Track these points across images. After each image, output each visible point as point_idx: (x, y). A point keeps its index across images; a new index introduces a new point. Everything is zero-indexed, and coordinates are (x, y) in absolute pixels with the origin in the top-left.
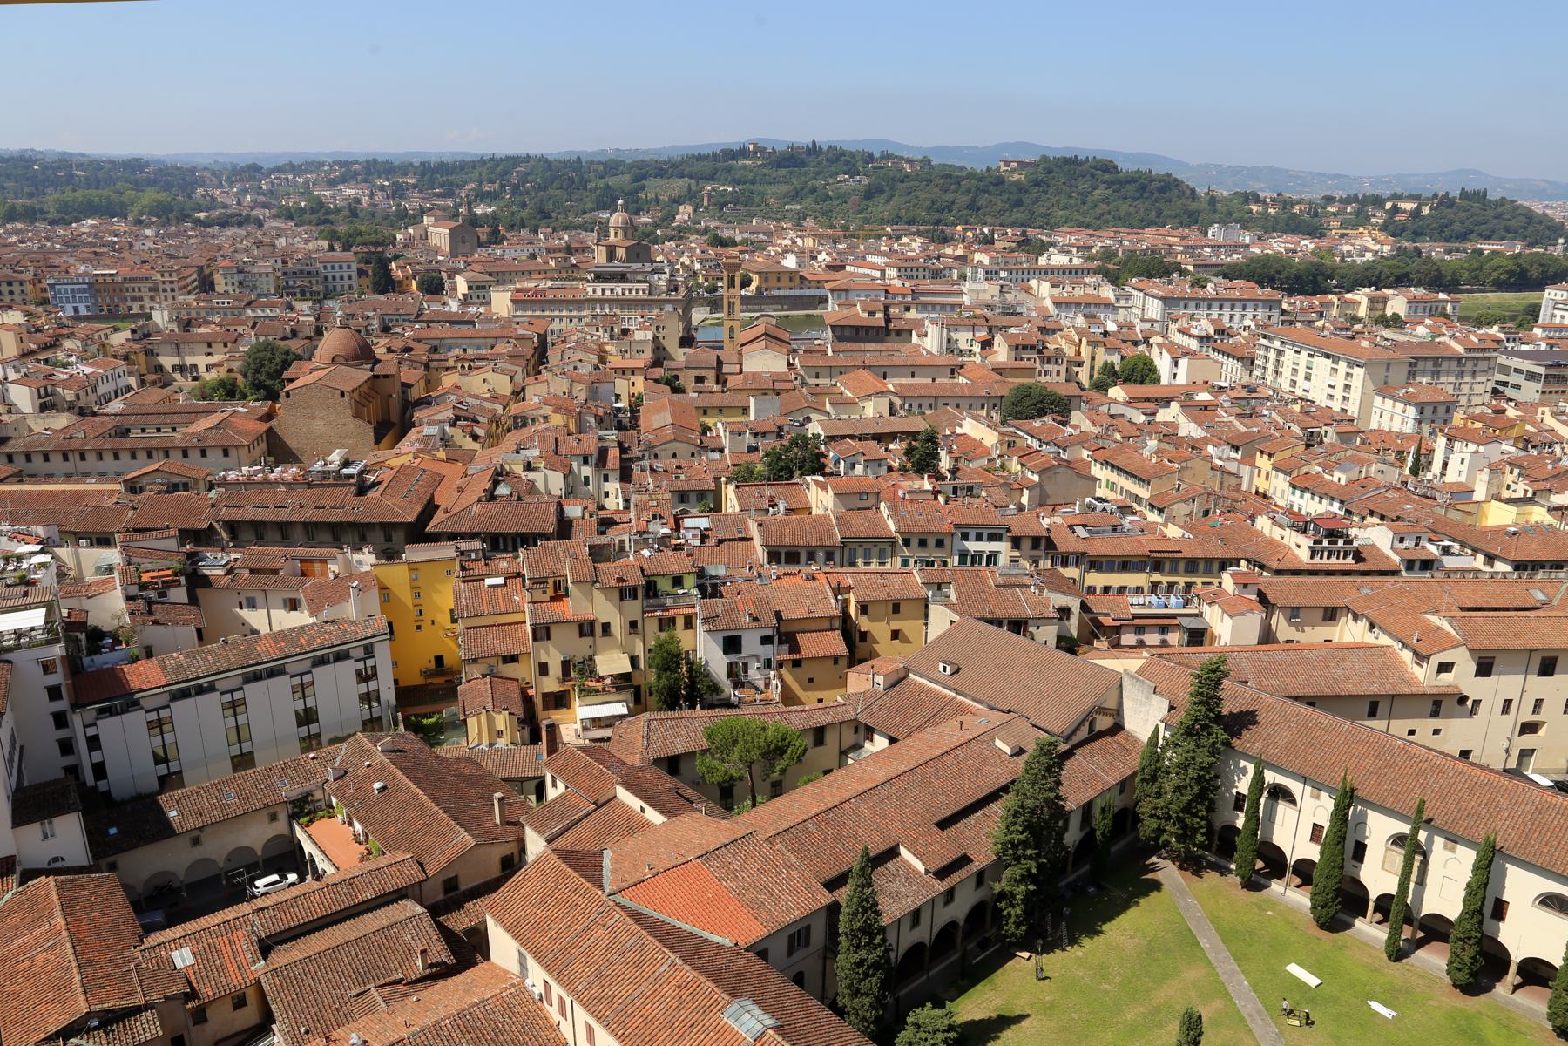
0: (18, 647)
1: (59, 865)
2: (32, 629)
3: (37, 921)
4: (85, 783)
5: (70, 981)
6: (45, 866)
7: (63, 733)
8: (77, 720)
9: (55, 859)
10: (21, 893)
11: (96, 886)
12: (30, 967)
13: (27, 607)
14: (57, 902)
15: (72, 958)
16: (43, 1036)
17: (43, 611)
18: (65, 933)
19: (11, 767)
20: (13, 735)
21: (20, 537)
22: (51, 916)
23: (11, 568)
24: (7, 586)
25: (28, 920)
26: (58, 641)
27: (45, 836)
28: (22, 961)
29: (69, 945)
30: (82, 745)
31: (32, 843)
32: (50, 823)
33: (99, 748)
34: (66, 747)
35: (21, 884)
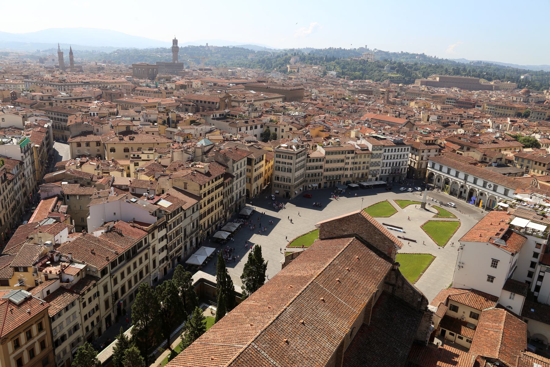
0: (532, 235)
1: (510, 309)
2: (539, 231)
3: (495, 321)
4: (530, 290)
5: (497, 345)
6: (506, 307)
7: (532, 270)
8: (539, 268)
9: (510, 307)
10: (495, 310)
11: (518, 323)
12: (487, 333)
13: (541, 223)
14: (504, 320)
15: (501, 339)
16: (481, 355)
17: (546, 227)
18: (502, 331)
19: (511, 271)
20: (516, 261)
21: (547, 201)
22: (500, 322)
23: (540, 209)
24: (537, 214)
25: (493, 319)
26: (546, 239)
27: (510, 298)
28: (486, 330)
29: (501, 335)
30: (536, 277)
31: (506, 297)
32: (514, 295)
33: (542, 281)
34: (530, 275)
35: (496, 307)
